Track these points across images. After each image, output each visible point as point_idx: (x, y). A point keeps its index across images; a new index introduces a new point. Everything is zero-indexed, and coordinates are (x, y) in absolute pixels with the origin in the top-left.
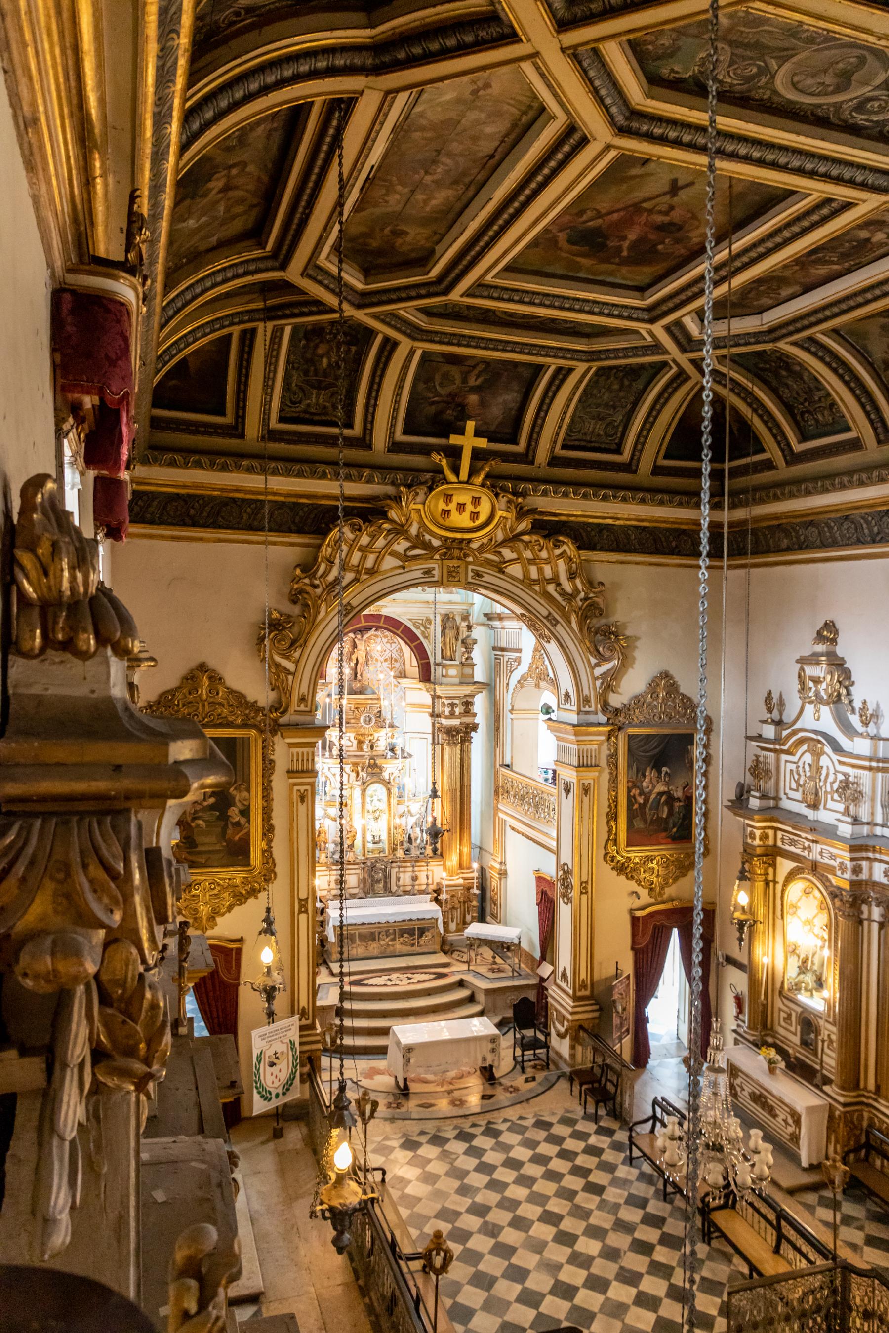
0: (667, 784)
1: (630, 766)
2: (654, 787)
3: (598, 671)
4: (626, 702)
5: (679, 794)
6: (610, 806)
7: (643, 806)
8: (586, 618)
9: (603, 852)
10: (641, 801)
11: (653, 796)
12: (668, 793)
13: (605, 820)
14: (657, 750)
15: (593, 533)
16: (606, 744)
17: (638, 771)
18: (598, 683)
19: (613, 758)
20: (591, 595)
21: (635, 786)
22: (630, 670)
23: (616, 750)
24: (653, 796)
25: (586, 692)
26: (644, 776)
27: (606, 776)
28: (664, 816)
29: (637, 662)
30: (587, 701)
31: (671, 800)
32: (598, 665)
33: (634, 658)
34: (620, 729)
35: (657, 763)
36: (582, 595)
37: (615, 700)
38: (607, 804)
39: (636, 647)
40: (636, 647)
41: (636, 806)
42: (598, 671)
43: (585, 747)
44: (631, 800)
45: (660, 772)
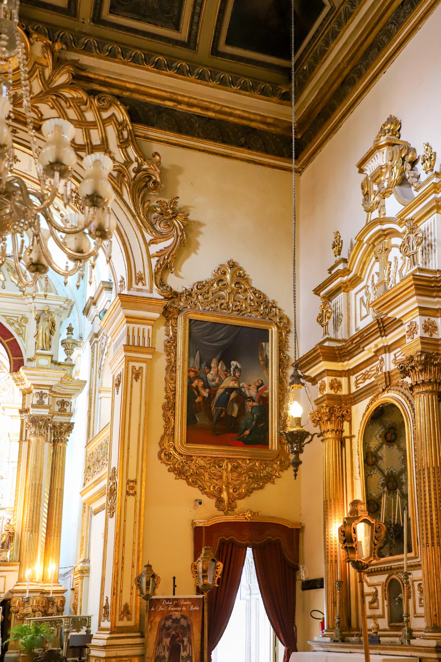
0: (237, 380)
1: (191, 354)
2: (221, 381)
3: (154, 249)
4: (189, 288)
5: (252, 392)
6: (167, 398)
7: (207, 401)
8: (140, 191)
9: (159, 449)
10: (206, 394)
11: (220, 391)
12: (238, 390)
13: (162, 412)
14: (226, 341)
15: (151, 113)
16: (163, 328)
17: (201, 363)
18: (154, 261)
19: (172, 343)
20: (145, 166)
21: (197, 377)
22: (193, 255)
23: (175, 333)
24: (220, 391)
25: (139, 269)
26: (210, 368)
27: (161, 363)
28: (235, 414)
29: (200, 247)
30: (140, 279)
31: (242, 398)
32: (153, 242)
33: (197, 244)
34: (180, 312)
35: (226, 357)
36: (135, 165)
37: (175, 282)
38: (164, 394)
39: (200, 233)
40: (200, 233)
41: (198, 399)
42: (154, 249)
43: (136, 326)
44: (192, 393)
45: (228, 366)
